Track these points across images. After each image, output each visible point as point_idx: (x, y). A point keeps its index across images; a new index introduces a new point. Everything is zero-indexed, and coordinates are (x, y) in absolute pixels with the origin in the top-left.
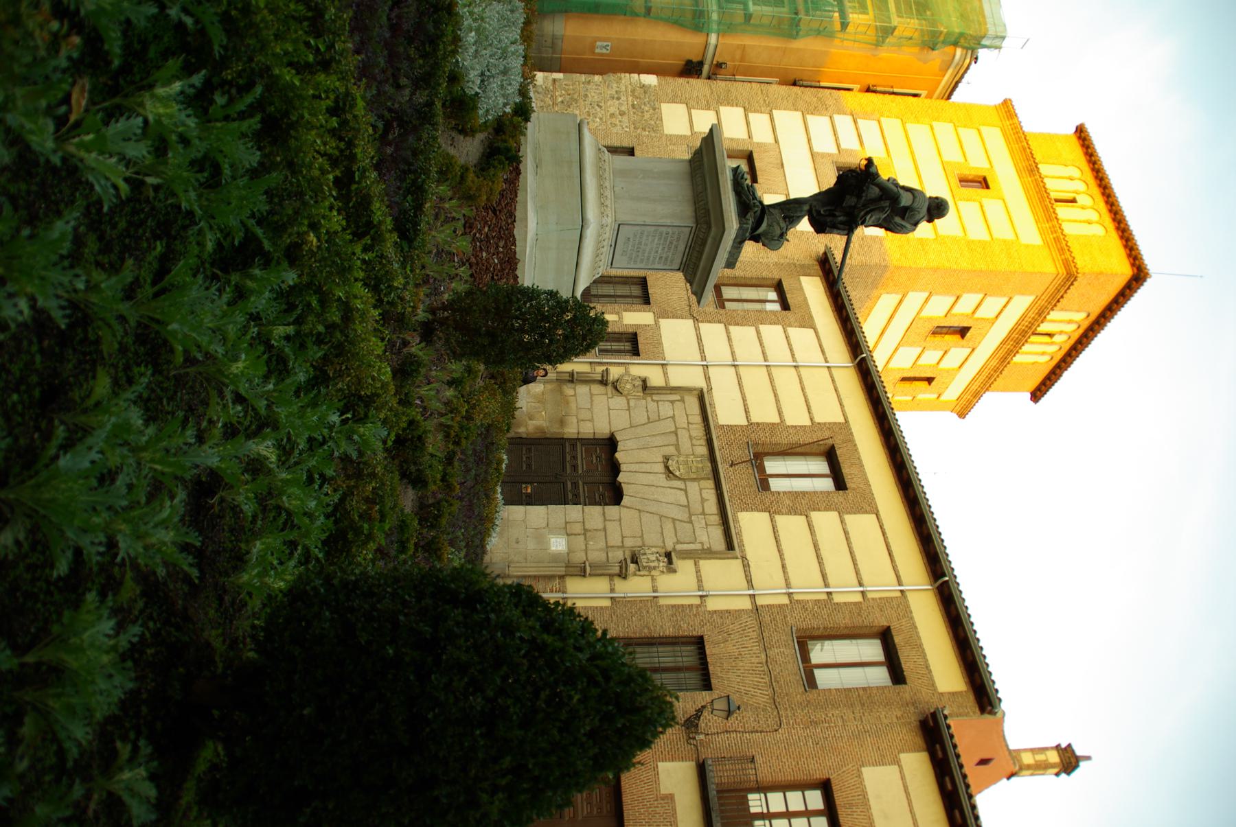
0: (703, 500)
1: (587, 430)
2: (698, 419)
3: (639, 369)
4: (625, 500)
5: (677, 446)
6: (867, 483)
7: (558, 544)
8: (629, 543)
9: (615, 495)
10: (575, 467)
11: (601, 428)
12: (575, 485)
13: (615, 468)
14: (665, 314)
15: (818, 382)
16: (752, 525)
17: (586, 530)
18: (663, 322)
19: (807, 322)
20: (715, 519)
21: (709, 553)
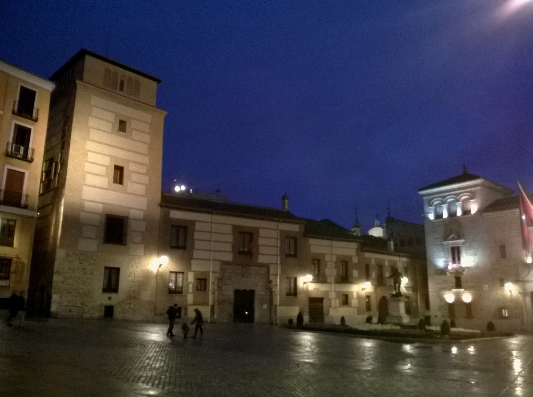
1: (232, 297)
4: (254, 289)
5: (239, 274)
7: (265, 306)
9: (252, 292)
16: (261, 259)
19: (193, 223)
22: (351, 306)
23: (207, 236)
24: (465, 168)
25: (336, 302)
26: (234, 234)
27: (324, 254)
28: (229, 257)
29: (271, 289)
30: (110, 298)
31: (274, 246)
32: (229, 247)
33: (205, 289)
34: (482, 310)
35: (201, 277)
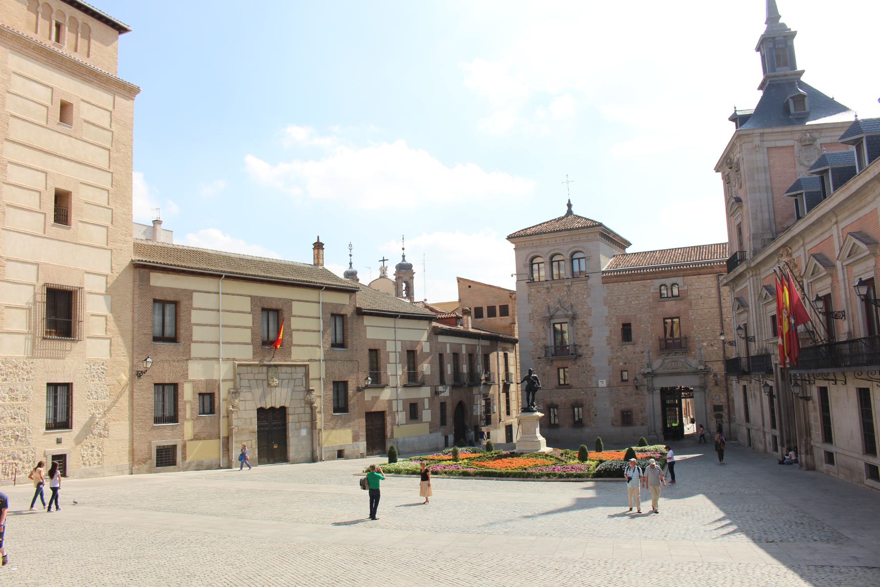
0: (286, 373)
1: (255, 421)
2: (249, 368)
3: (223, 392)
4: (287, 405)
5: (263, 380)
6: (280, 299)
7: (304, 432)
8: (303, 405)
10: (267, 426)
11: (254, 414)
12: (275, 426)
13: (272, 408)
14: (185, 376)
15: (226, 302)
16: (298, 355)
17: (299, 422)
18: (190, 377)
20: (293, 369)
21: (307, 375)
22: (421, 422)
23: (210, 318)
24: (569, 205)
25: (401, 417)
26: (252, 312)
27: (385, 341)
28: (246, 354)
29: (312, 403)
30: (59, 441)
31: (314, 331)
32: (247, 336)
33: (212, 411)
34: (596, 415)
35: (203, 391)
